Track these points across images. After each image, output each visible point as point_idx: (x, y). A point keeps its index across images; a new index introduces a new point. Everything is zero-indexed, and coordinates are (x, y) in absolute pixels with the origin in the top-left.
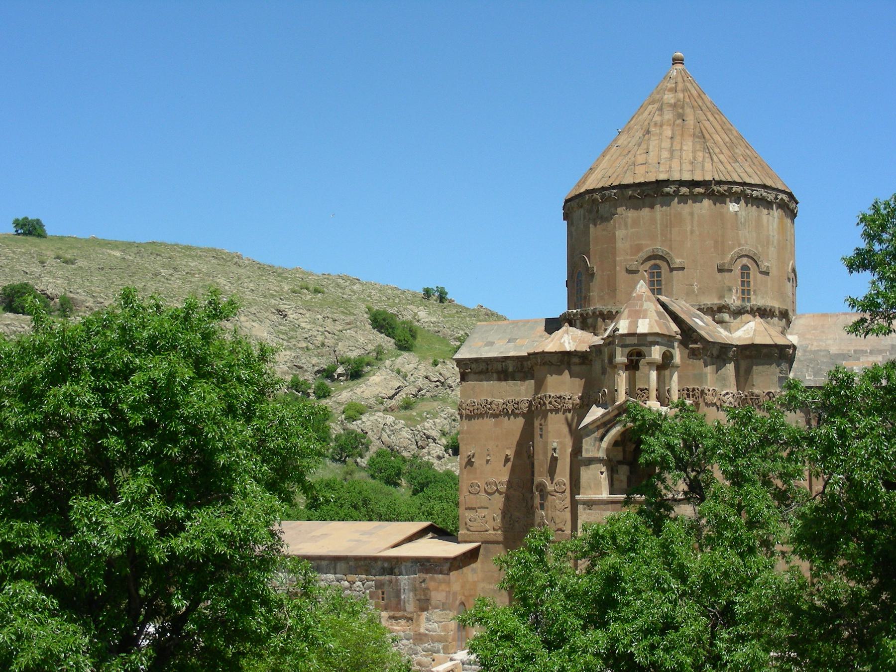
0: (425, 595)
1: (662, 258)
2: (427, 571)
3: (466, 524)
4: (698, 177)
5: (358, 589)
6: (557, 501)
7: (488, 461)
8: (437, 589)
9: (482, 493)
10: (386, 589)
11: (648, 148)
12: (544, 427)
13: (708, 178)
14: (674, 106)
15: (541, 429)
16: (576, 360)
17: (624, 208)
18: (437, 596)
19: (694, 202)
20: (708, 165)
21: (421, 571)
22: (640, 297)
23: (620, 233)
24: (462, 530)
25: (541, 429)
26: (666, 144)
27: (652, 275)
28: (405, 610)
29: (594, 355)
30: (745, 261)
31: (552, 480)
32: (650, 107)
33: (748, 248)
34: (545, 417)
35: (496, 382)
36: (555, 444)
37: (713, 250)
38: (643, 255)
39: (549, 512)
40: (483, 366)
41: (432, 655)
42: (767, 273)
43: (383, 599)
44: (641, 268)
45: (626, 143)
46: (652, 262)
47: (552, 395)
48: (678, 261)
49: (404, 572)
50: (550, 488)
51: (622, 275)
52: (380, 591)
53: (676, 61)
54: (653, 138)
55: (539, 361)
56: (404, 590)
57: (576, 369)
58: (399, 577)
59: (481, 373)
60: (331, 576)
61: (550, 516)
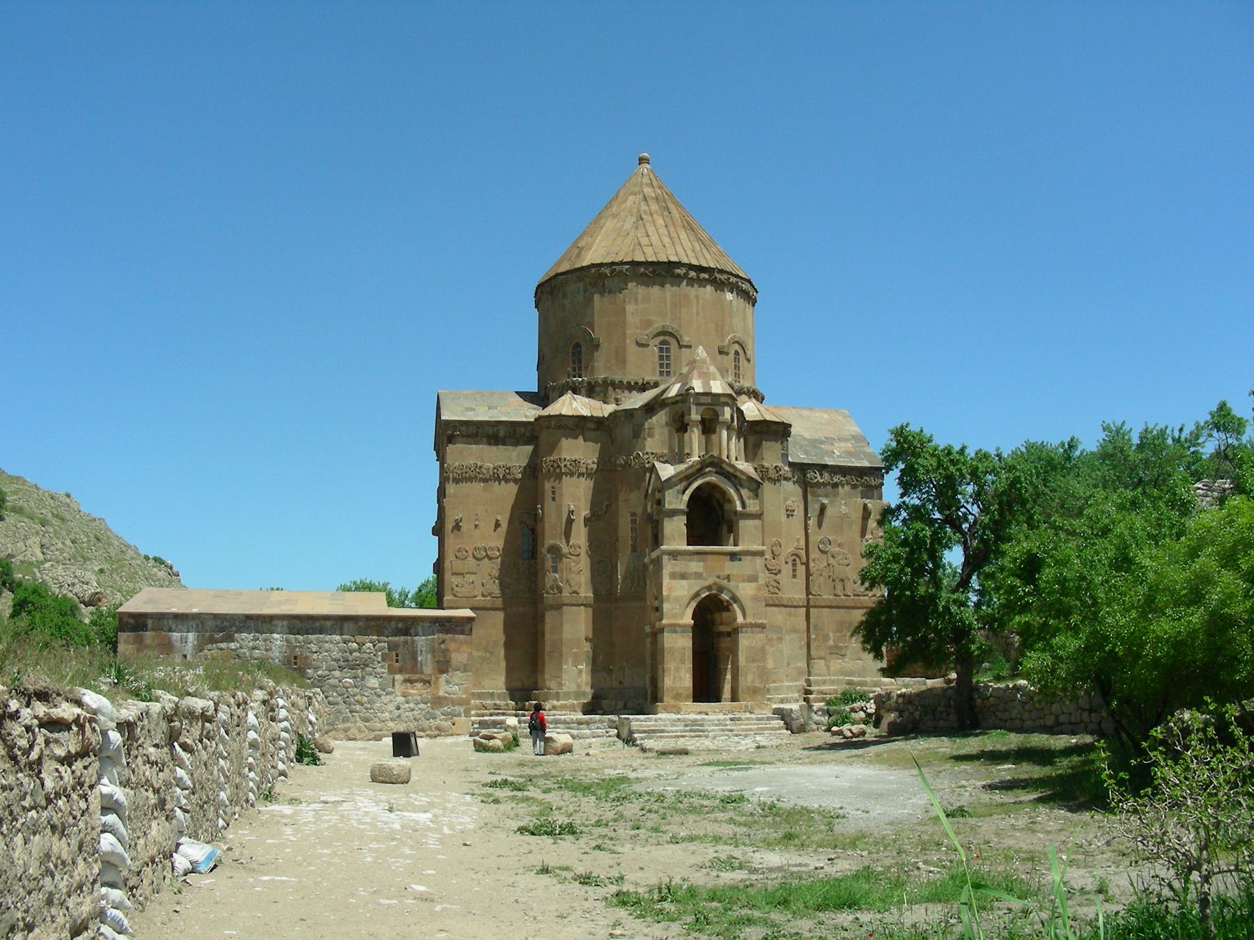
0: (445, 656)
1: (671, 335)
2: (447, 632)
3: (452, 589)
4: (705, 265)
5: (368, 651)
6: (572, 564)
7: (476, 526)
8: (457, 650)
9: (471, 559)
10: (400, 650)
11: (647, 233)
12: (557, 491)
13: (712, 266)
14: (657, 199)
15: (554, 492)
16: (592, 426)
17: (635, 284)
18: (458, 657)
19: (700, 287)
20: (707, 255)
21: (440, 631)
22: (704, 361)
23: (630, 308)
24: (448, 595)
25: (554, 492)
26: (663, 231)
27: (661, 350)
28: (422, 673)
29: (623, 420)
30: (737, 347)
31: (568, 542)
32: (631, 198)
33: (738, 335)
34: (560, 480)
35: (485, 446)
36: (572, 507)
37: (714, 332)
38: (652, 330)
39: (564, 574)
40: (472, 430)
41: (452, 718)
42: (749, 360)
43: (397, 661)
44: (652, 343)
45: (619, 225)
46: (661, 338)
47: (568, 458)
48: (686, 339)
49: (421, 633)
50: (565, 550)
51: (632, 349)
52: (394, 653)
53: (642, 161)
54: (648, 225)
55: (553, 424)
56: (421, 651)
57: (591, 434)
58: (416, 638)
59: (468, 436)
60: (337, 638)
61: (565, 579)
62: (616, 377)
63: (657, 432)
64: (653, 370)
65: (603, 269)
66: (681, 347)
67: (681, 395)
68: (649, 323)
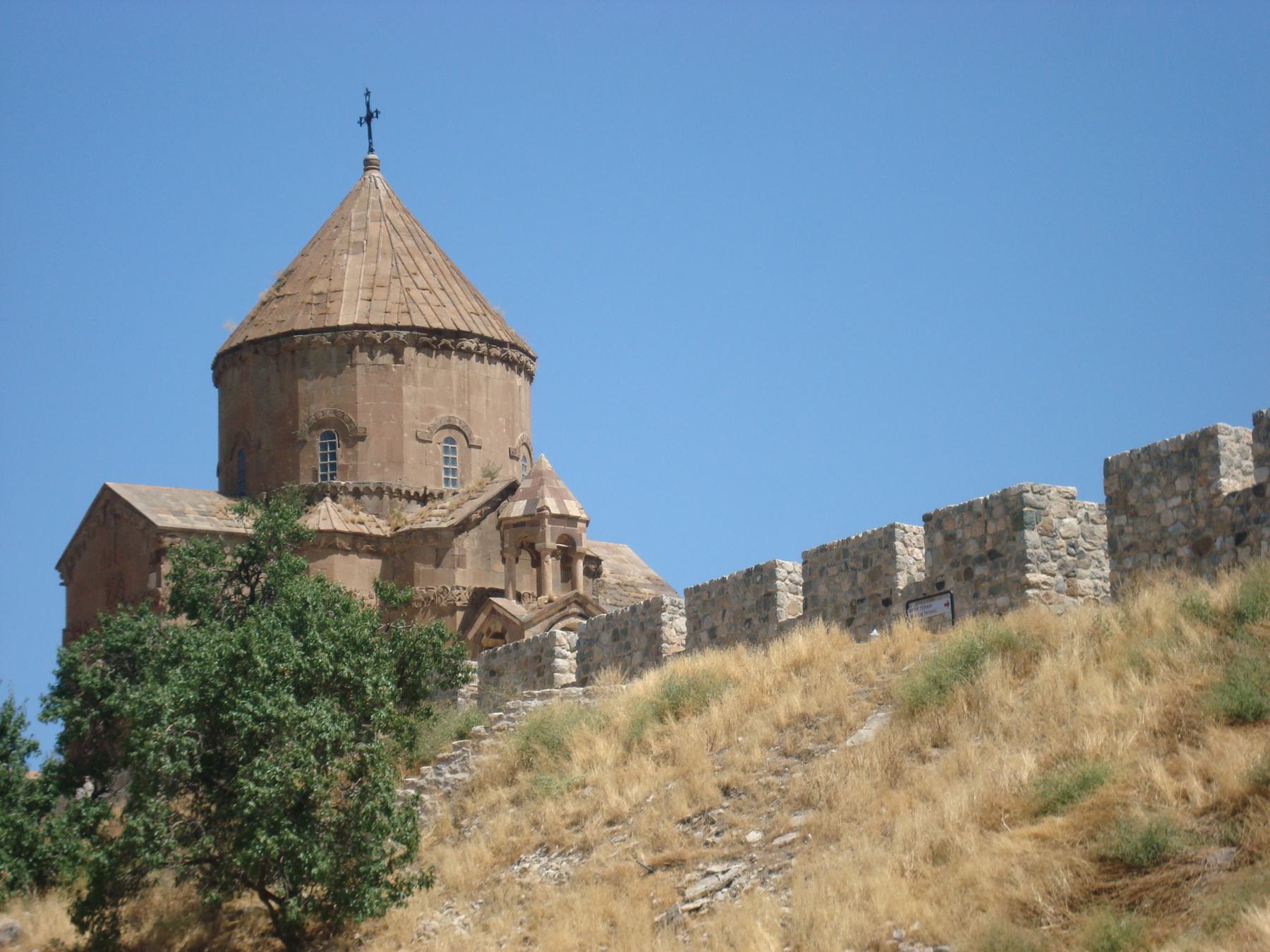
23: (407, 390)
55: (323, 542)
62: (394, 483)
63: (469, 559)
64: (438, 476)
65: (370, 332)
66: (470, 446)
67: (532, 515)
68: (432, 413)
